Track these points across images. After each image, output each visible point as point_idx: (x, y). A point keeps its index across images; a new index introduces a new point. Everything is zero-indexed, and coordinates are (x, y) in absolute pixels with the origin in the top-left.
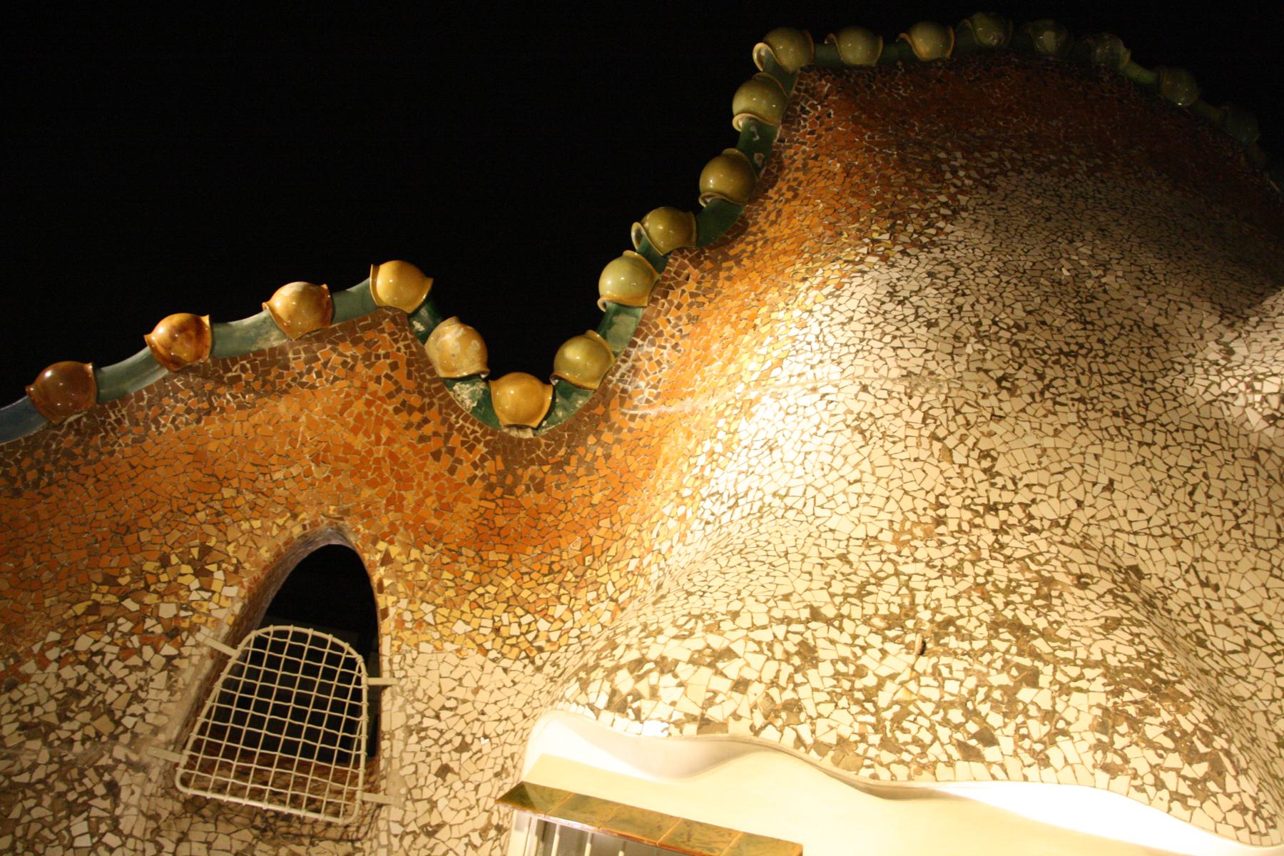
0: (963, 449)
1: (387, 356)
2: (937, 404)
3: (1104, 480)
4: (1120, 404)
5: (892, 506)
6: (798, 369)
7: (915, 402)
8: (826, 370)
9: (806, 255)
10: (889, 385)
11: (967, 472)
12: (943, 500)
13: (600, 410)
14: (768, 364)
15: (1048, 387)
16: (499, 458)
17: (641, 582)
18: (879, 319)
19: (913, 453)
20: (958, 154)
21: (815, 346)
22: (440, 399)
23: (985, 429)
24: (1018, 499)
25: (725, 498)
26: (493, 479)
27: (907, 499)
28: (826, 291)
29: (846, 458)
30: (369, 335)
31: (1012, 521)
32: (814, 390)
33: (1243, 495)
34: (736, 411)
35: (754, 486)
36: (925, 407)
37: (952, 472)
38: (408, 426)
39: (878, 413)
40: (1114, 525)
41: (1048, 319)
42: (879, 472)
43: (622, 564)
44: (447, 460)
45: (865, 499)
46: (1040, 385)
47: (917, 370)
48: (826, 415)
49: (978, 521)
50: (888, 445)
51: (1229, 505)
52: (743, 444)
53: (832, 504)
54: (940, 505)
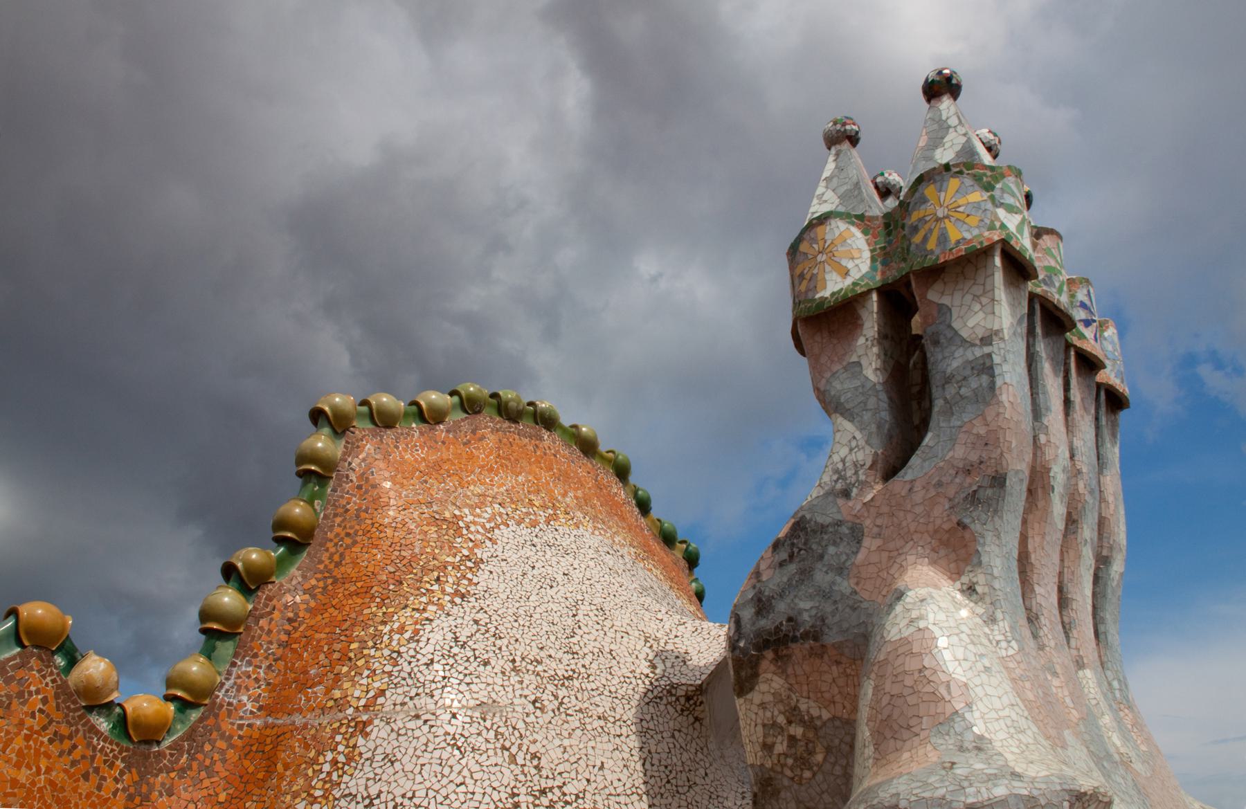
0: (521, 754)
1: (38, 692)
2: (501, 724)
3: (599, 764)
4: (601, 710)
5: (487, 799)
6: (399, 699)
7: (488, 724)
8: (423, 701)
9: (378, 600)
10: (469, 713)
11: (526, 769)
12: (515, 791)
13: (211, 721)
14: (371, 694)
15: (561, 703)
16: (134, 770)
18: (451, 661)
19: (493, 760)
20: (466, 511)
21: (410, 682)
22: (83, 725)
23: (531, 738)
24: (557, 783)
25: (359, 798)
26: (132, 790)
27: (495, 793)
28: (407, 635)
29: (451, 767)
30: (21, 673)
31: (555, 799)
32: (417, 717)
33: (669, 761)
34: (351, 730)
35: (385, 789)
36: (495, 727)
37: (518, 771)
38: (61, 754)
39: (467, 734)
40: (607, 791)
41: (552, 652)
42: (476, 776)
44: (94, 779)
45: (470, 796)
46: (556, 703)
47: (485, 700)
48: (431, 736)
49: (537, 802)
50: (477, 757)
51: (662, 768)
52: (365, 756)
53: (448, 802)
54: (514, 795)
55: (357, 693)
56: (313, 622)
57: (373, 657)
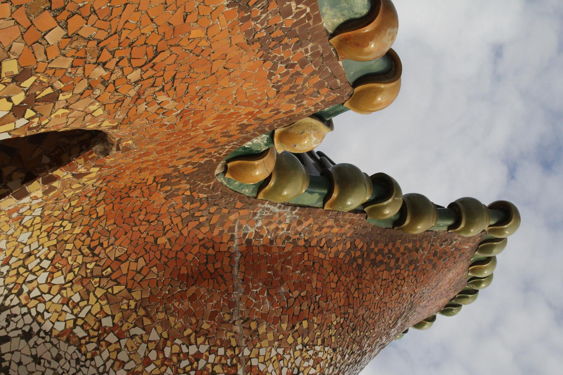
17: (91, 347)
43: (107, 309)
55: (263, 352)
56: (326, 265)
57: (295, 350)
